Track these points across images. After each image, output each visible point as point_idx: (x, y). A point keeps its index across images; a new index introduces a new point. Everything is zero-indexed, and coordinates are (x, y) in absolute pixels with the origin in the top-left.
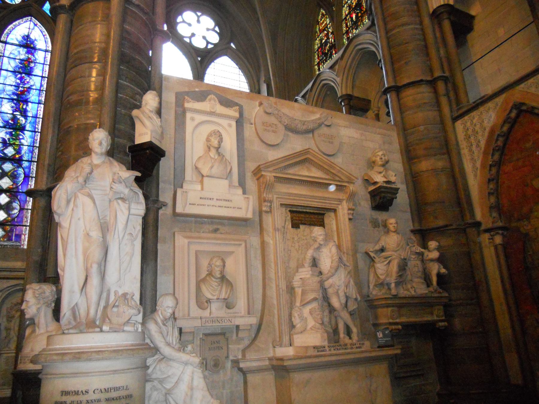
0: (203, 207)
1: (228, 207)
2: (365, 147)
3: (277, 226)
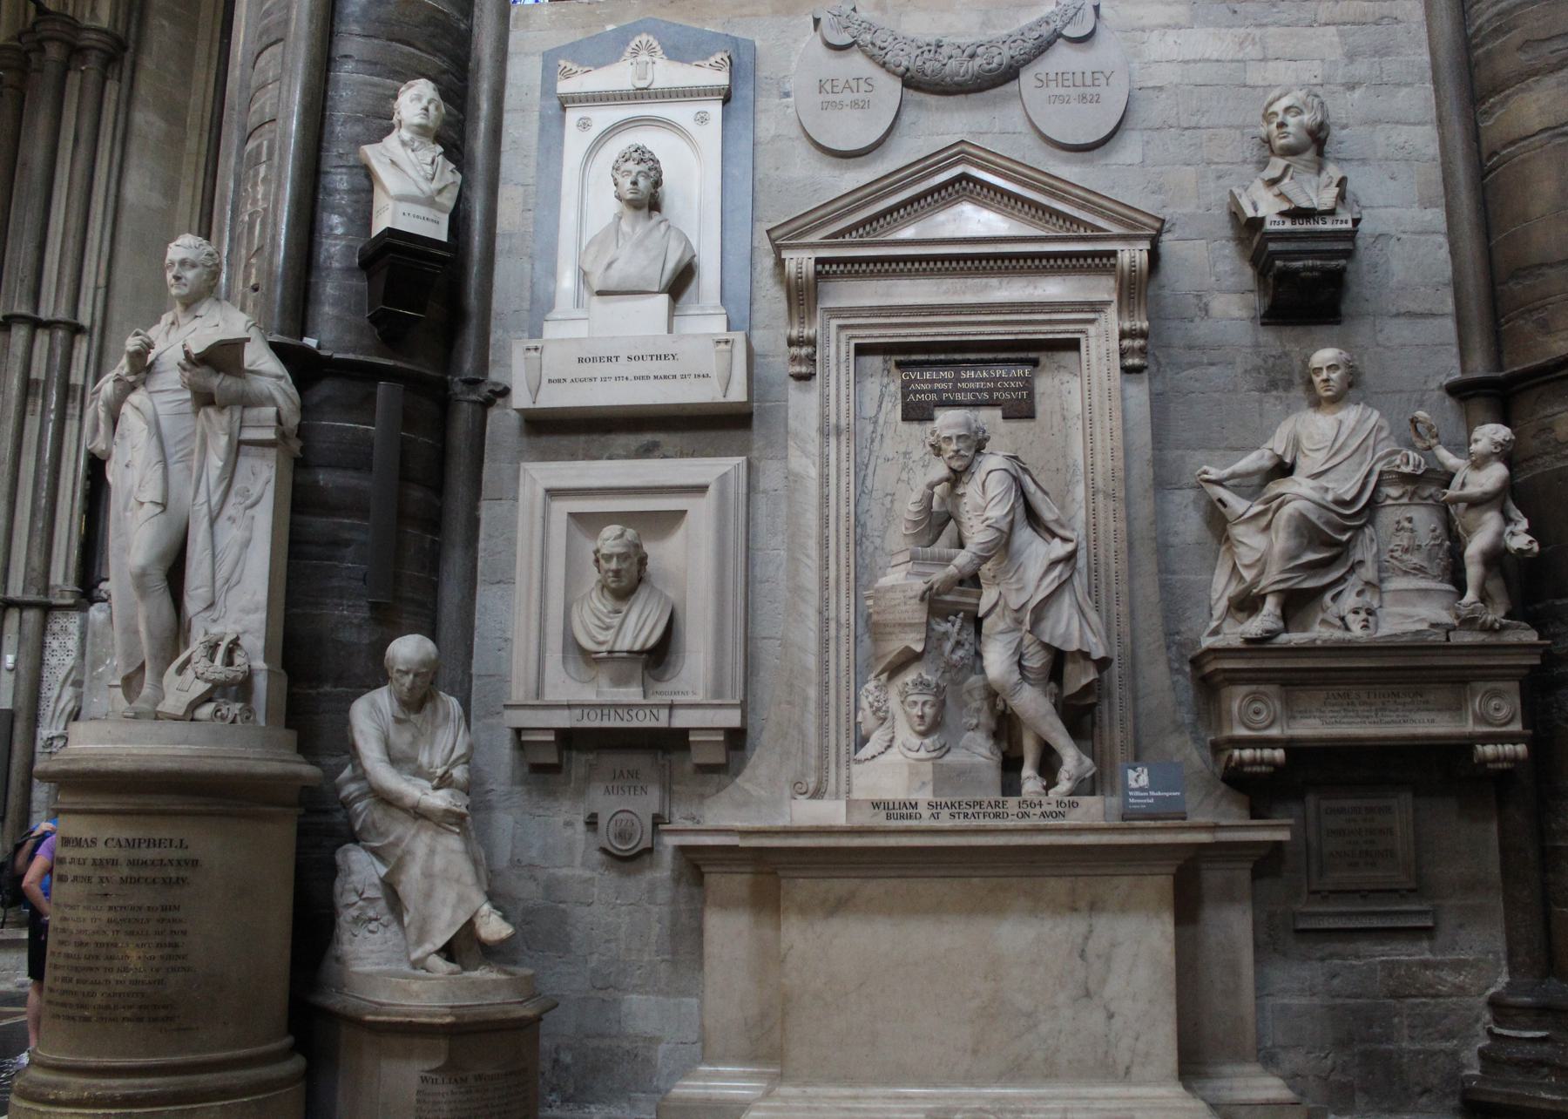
0: (587, 385)
1: (665, 377)
2: (1254, 87)
3: (833, 420)
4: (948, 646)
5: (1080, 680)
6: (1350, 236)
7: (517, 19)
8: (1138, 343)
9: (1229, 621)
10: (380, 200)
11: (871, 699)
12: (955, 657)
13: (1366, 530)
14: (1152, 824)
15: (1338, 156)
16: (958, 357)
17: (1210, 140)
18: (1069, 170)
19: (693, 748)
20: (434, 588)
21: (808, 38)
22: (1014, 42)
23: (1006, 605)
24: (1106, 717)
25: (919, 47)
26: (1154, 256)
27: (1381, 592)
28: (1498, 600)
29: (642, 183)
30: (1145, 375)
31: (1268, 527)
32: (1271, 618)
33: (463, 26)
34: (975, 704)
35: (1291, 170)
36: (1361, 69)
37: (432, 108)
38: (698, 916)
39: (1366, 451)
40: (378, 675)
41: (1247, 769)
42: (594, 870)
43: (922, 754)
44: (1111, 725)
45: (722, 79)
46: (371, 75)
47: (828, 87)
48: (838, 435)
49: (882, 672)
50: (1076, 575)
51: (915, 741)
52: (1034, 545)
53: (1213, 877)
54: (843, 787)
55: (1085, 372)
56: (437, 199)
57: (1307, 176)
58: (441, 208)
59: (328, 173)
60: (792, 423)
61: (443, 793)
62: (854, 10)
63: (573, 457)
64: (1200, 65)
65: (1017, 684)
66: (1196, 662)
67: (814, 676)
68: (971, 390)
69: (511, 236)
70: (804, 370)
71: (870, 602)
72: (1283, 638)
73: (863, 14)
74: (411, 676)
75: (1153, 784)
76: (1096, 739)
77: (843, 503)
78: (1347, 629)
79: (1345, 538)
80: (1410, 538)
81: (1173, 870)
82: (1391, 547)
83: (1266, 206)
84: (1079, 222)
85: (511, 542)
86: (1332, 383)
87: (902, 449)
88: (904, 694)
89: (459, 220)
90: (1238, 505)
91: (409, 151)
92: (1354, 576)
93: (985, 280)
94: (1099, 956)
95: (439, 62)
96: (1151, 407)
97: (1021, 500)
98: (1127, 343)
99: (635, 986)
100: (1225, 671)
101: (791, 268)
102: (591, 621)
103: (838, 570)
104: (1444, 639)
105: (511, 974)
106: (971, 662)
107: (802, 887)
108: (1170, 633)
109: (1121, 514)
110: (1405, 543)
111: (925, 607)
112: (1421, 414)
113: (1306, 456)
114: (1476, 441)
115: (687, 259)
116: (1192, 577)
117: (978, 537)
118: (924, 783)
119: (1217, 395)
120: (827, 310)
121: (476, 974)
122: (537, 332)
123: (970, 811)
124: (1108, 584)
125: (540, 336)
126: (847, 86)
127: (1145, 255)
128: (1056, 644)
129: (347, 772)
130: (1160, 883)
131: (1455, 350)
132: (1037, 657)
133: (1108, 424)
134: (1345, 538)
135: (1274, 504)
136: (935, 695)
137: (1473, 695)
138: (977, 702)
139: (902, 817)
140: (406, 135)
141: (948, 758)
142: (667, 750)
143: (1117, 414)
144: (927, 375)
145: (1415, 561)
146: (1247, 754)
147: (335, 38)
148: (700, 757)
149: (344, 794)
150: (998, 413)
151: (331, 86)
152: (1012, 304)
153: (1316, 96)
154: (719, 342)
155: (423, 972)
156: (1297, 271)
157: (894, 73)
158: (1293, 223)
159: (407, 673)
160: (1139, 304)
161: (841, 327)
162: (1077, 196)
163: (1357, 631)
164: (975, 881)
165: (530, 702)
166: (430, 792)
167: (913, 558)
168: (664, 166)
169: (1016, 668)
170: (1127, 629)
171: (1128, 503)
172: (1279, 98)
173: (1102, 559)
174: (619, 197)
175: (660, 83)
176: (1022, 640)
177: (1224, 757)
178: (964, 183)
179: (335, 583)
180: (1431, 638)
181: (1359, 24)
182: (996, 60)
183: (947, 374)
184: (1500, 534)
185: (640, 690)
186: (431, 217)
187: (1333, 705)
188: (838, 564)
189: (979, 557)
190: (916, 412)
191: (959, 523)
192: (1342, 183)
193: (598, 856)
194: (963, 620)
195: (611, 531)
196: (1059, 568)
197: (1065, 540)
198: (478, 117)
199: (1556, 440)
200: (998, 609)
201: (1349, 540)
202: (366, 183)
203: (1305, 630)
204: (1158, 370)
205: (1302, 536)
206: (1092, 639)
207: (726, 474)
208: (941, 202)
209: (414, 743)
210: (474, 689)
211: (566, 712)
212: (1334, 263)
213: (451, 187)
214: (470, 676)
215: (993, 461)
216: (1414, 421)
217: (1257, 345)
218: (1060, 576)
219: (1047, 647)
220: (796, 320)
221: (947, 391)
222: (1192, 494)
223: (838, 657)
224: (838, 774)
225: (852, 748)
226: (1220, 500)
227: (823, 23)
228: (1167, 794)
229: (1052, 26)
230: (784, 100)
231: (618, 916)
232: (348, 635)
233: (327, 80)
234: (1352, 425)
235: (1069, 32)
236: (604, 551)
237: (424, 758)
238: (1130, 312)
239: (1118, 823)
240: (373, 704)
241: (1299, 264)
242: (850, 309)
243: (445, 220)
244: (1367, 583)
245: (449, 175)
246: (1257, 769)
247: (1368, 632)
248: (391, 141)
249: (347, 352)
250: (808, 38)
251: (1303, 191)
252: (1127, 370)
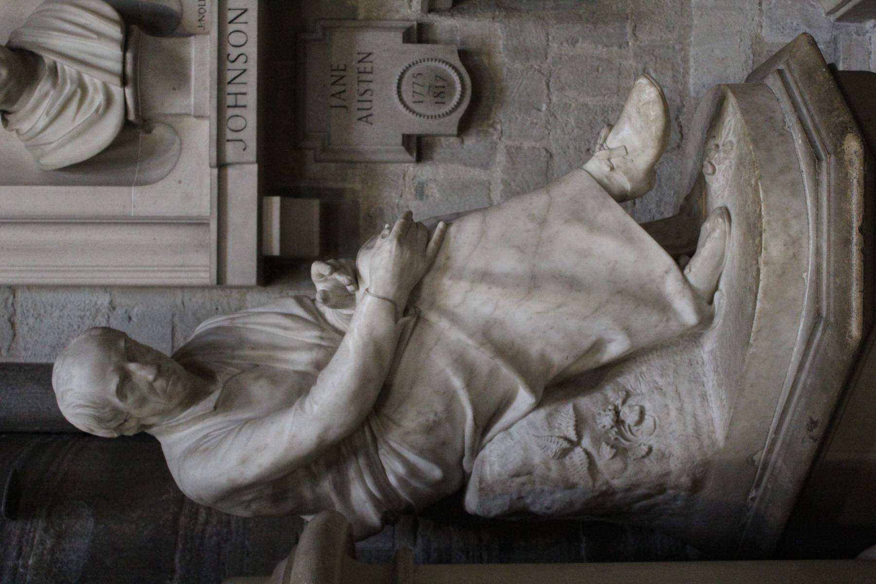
42: (494, 148)
102: (71, 120)
193: (471, 141)
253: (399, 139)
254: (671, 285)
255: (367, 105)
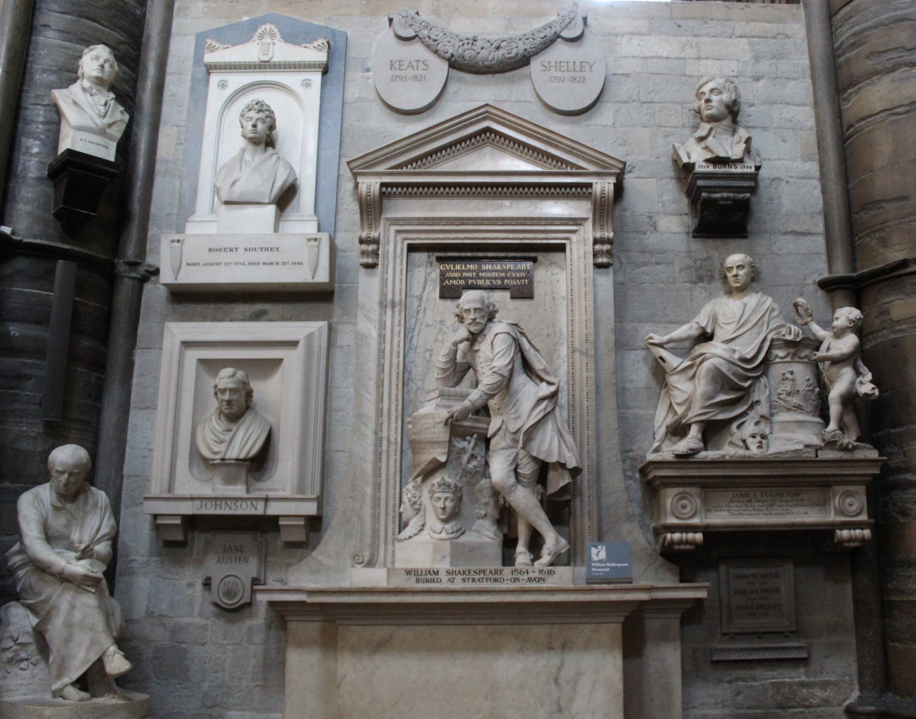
0: (215, 268)
1: (271, 264)
2: (691, 76)
3: (390, 297)
4: (465, 458)
5: (558, 484)
6: (754, 177)
7: (179, 10)
8: (606, 247)
9: (667, 442)
10: (65, 130)
11: (409, 495)
12: (471, 466)
13: (762, 380)
14: (606, 586)
15: (747, 124)
16: (480, 254)
17: (661, 111)
18: (563, 128)
19: (282, 530)
20: (98, 412)
21: (384, 32)
22: (527, 39)
23: (507, 429)
24: (578, 509)
25: (461, 41)
26: (619, 188)
27: (771, 423)
28: (851, 429)
29: (260, 126)
30: (611, 270)
31: (693, 377)
32: (695, 441)
33: (138, 12)
34: (484, 500)
35: (714, 131)
36: (764, 67)
37: (107, 66)
38: (282, 652)
39: (762, 326)
40: (43, 476)
41: (676, 547)
43: (444, 535)
44: (582, 515)
45: (322, 57)
46: (64, 40)
47: (397, 65)
48: (393, 307)
49: (417, 476)
50: (557, 409)
51: (439, 526)
52: (527, 387)
53: (653, 624)
54: (389, 559)
55: (569, 266)
56: (108, 130)
57: (724, 136)
58: (111, 138)
59: (26, 109)
60: (361, 298)
61: (84, 562)
62: (417, 13)
63: (204, 319)
64: (655, 60)
65: (513, 486)
66: (643, 471)
67: (370, 479)
68: (489, 278)
69: (167, 161)
70: (370, 261)
71: (410, 426)
72: (703, 455)
73: (424, 17)
74: (66, 475)
75: (610, 558)
76: (572, 525)
77: (395, 356)
78: (747, 448)
79: (746, 384)
80: (792, 386)
81: (622, 619)
82: (779, 391)
83: (696, 156)
84: (567, 163)
85: (156, 380)
86: (739, 278)
87: (439, 319)
88: (432, 492)
89: (126, 146)
90: (673, 361)
91: (88, 96)
92: (753, 411)
93: (500, 202)
94: (568, 682)
95: (118, 35)
96: (615, 292)
97: (519, 355)
98: (598, 247)
99: (236, 704)
100: (661, 477)
101: (363, 188)
102: (210, 437)
103: (390, 403)
104: (814, 456)
105: (130, 699)
106: (481, 470)
107: (354, 632)
108: (625, 452)
109: (592, 366)
110: (788, 389)
111: (448, 429)
112: (801, 300)
113: (721, 328)
114: (837, 319)
115: (290, 181)
116: (641, 412)
117: (487, 379)
118: (444, 557)
119: (661, 285)
120: (387, 219)
121: (99, 700)
122: (181, 229)
123: (476, 577)
124: (581, 415)
125: (183, 232)
126: (410, 65)
127: (612, 187)
128: (542, 457)
129: (16, 547)
130: (612, 629)
131: (824, 258)
132: (529, 466)
133: (583, 303)
134: (746, 384)
135: (698, 361)
136: (454, 493)
137: (834, 495)
138: (486, 498)
139: (427, 581)
140: (87, 84)
141: (463, 539)
142: (263, 532)
143: (590, 296)
144: (458, 267)
145: (795, 401)
146: (677, 536)
147: (37, 13)
148: (286, 536)
149: (10, 563)
150: (507, 294)
151: (31, 47)
152: (519, 219)
153: (732, 82)
154: (310, 240)
155: (60, 700)
156: (716, 201)
157: (443, 58)
158: (714, 167)
159: (63, 473)
160: (607, 220)
161: (398, 232)
162: (566, 145)
163: (754, 450)
164: (480, 628)
165: (164, 496)
166: (74, 562)
167: (442, 395)
168: (277, 116)
169: (513, 474)
170: (594, 447)
171: (596, 360)
172: (706, 83)
173: (577, 397)
174: (244, 136)
175: (278, 58)
176: (517, 455)
177: (661, 539)
178: (488, 134)
179: (16, 406)
180: (804, 455)
181: (762, 37)
182: (514, 51)
183: (471, 267)
184: (853, 383)
185: (244, 487)
186: (103, 143)
187: (738, 502)
188: (390, 398)
189: (487, 394)
190: (449, 293)
191: (475, 371)
192: (748, 141)
194: (477, 439)
195: (227, 372)
196: (545, 403)
197: (550, 383)
198: (146, 77)
199: (891, 319)
200: (501, 432)
201: (750, 386)
202: (55, 117)
203: (718, 449)
204: (621, 267)
205: (716, 383)
206: (567, 454)
207: (312, 333)
208: (471, 147)
209: (68, 525)
210: (124, 486)
211: (189, 503)
212: (741, 196)
213: (118, 124)
214: (122, 477)
215: (499, 327)
216: (796, 305)
217: (689, 251)
218: (545, 409)
219: (535, 459)
220: (366, 226)
221: (472, 278)
222: (642, 353)
223: (388, 465)
224: (386, 549)
225: (397, 530)
226: (661, 358)
227: (395, 22)
228: (619, 565)
229: (553, 30)
230: (366, 74)
231: (225, 652)
232: (26, 445)
233: (29, 42)
234: (753, 308)
235: (566, 34)
236: (220, 386)
237: (75, 536)
238: (601, 226)
239: (586, 586)
240: (37, 497)
241: (718, 195)
242: (405, 219)
243: (113, 146)
244: (762, 417)
245: (119, 115)
246: (683, 547)
247: (761, 450)
248: (75, 88)
249: (35, 238)
250: (384, 32)
251: (721, 145)
252: (598, 266)
253: (210, 575)
254: (66, 680)
255: (225, 560)
